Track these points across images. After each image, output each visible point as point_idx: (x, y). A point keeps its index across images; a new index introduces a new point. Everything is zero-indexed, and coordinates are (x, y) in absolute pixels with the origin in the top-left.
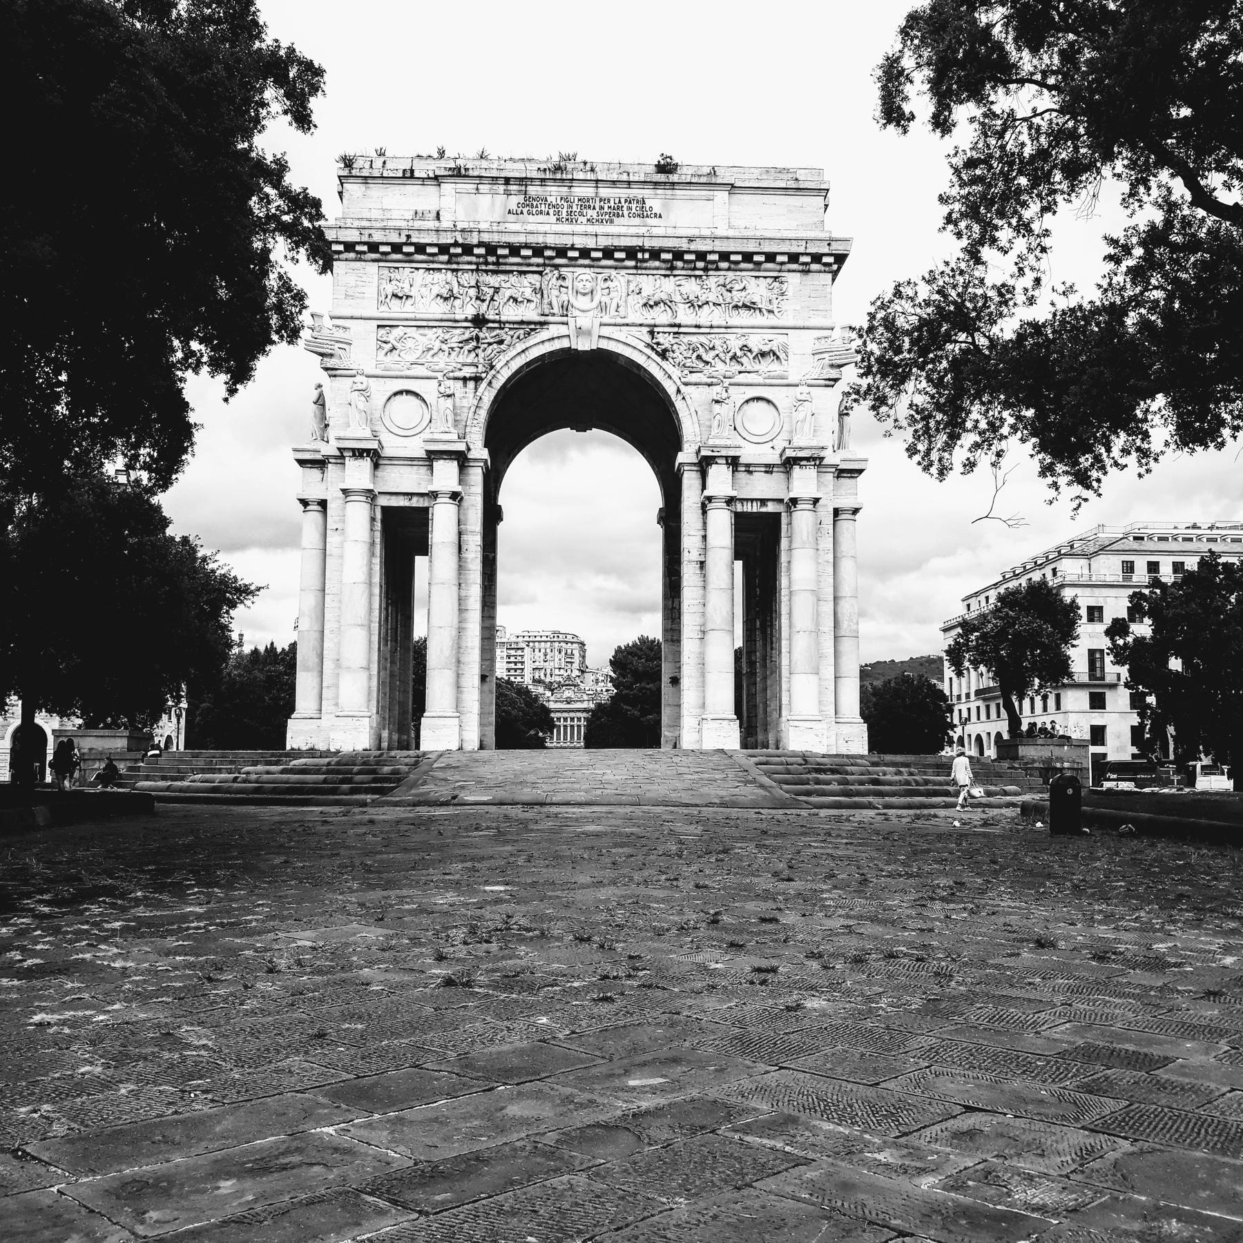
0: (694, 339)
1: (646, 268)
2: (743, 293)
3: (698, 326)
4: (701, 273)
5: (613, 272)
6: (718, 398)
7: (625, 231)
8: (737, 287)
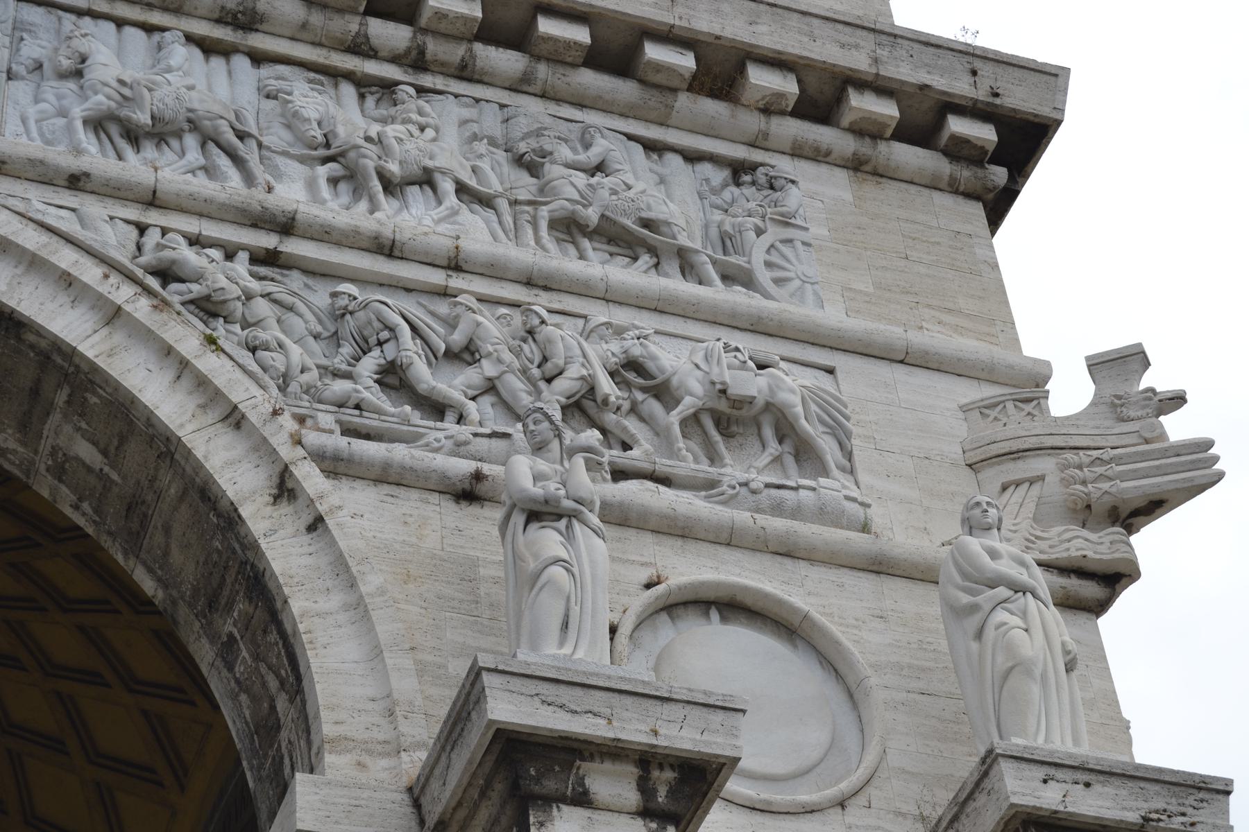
3: (388, 249)
4: (390, 72)
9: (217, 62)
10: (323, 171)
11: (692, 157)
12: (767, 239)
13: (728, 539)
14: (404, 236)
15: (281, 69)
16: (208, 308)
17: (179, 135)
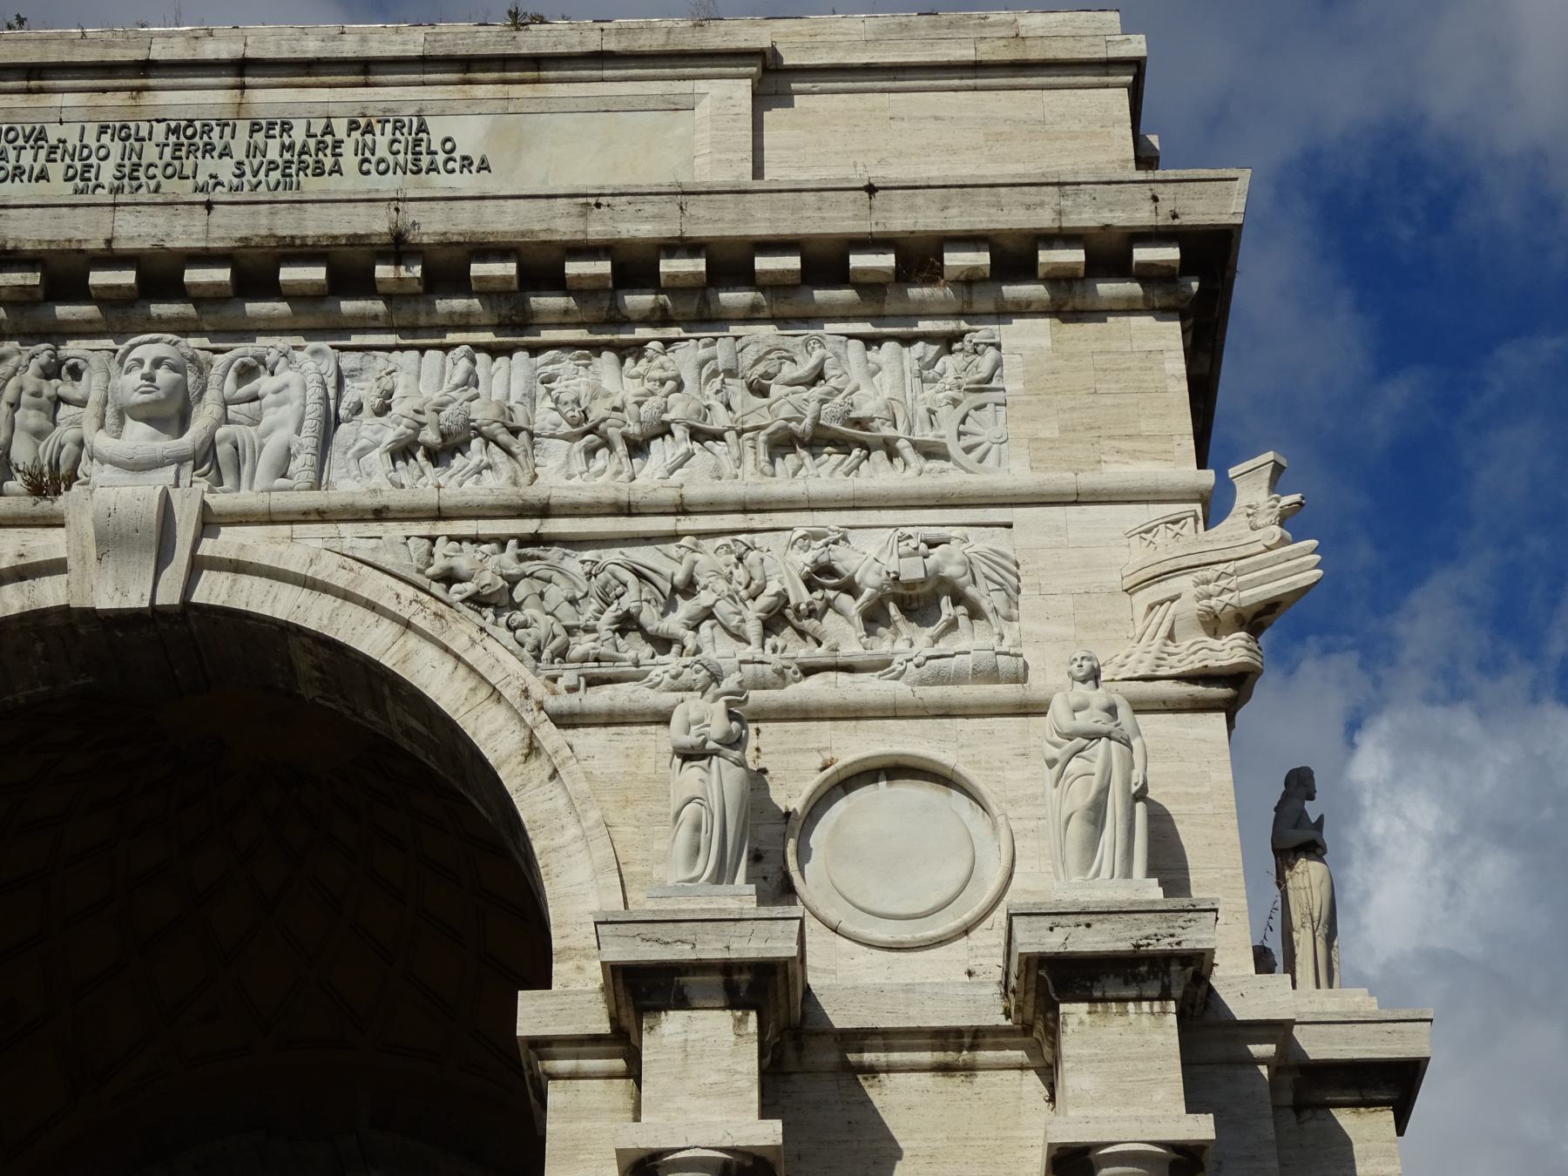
0: (611, 555)
2: (818, 391)
6: (691, 739)
8: (789, 371)
9: (502, 361)
11: (907, 341)
14: (636, 497)
15: (552, 353)
16: (477, 601)
17: (468, 443)
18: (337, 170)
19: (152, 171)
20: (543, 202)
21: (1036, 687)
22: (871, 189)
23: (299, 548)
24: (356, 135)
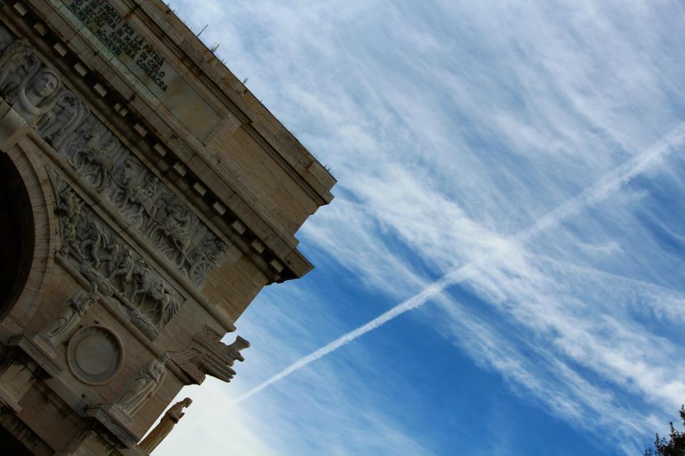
1: (112, 122)
2: (179, 227)
3: (114, 219)
4: (157, 173)
5: (81, 98)
7: (124, 72)
9: (123, 149)
10: (119, 190)
11: (209, 230)
12: (204, 262)
13: (122, 323)
17: (97, 165)
18: (133, 57)
19: (93, 16)
20: (166, 126)
21: (155, 345)
22: (235, 193)
23: (38, 162)
24: (145, 50)
